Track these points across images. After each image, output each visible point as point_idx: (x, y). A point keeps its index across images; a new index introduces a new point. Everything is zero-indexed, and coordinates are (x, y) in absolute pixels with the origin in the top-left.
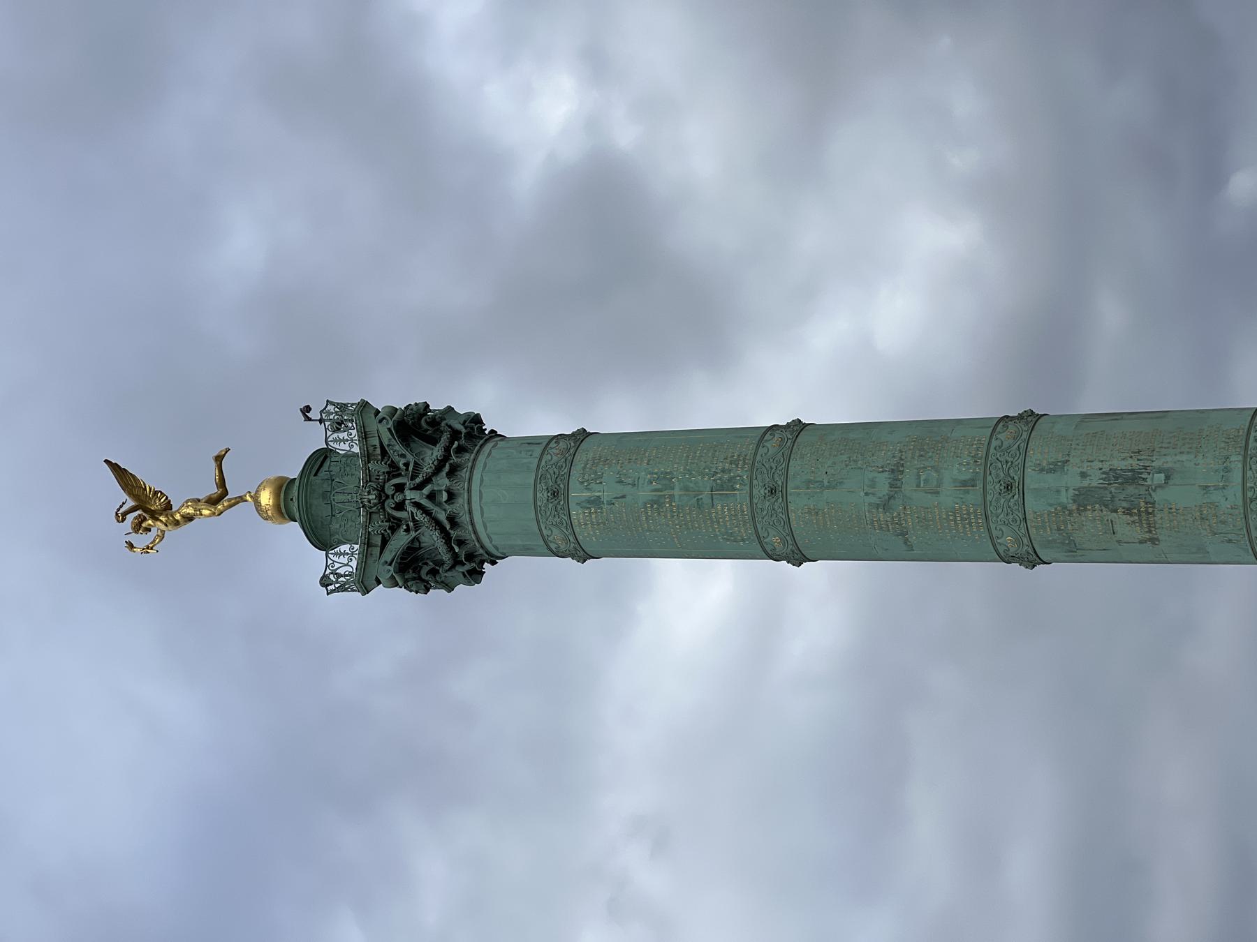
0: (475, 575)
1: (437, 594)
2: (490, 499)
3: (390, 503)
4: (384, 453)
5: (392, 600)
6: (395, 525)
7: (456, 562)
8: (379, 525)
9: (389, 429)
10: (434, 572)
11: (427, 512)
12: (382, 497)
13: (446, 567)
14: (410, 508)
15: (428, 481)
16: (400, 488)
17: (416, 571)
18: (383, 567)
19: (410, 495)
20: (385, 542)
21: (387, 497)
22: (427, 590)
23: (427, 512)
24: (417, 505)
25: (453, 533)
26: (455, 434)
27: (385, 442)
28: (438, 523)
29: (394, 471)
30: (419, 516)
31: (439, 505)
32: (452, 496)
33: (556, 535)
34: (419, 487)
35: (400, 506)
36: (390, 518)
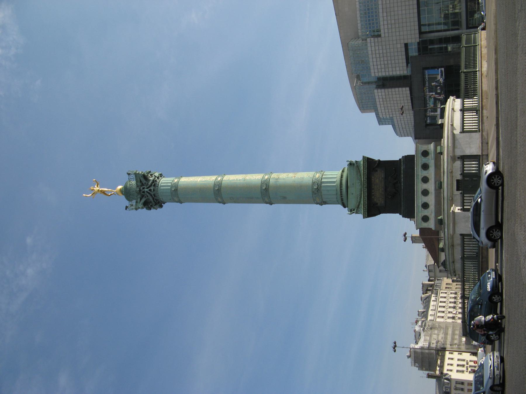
0: (161, 206)
1: (153, 210)
3: (141, 192)
4: (141, 181)
5: (144, 211)
6: (143, 196)
7: (156, 204)
8: (139, 196)
10: (152, 206)
11: (149, 193)
12: (140, 190)
15: (150, 187)
16: (144, 188)
17: (148, 205)
18: (140, 205)
19: (146, 190)
20: (141, 200)
22: (150, 209)
23: (149, 193)
24: (147, 192)
25: (155, 198)
26: (155, 177)
28: (151, 195)
29: (142, 185)
30: (148, 194)
32: (154, 190)
33: (176, 199)
34: (147, 188)
35: (144, 192)
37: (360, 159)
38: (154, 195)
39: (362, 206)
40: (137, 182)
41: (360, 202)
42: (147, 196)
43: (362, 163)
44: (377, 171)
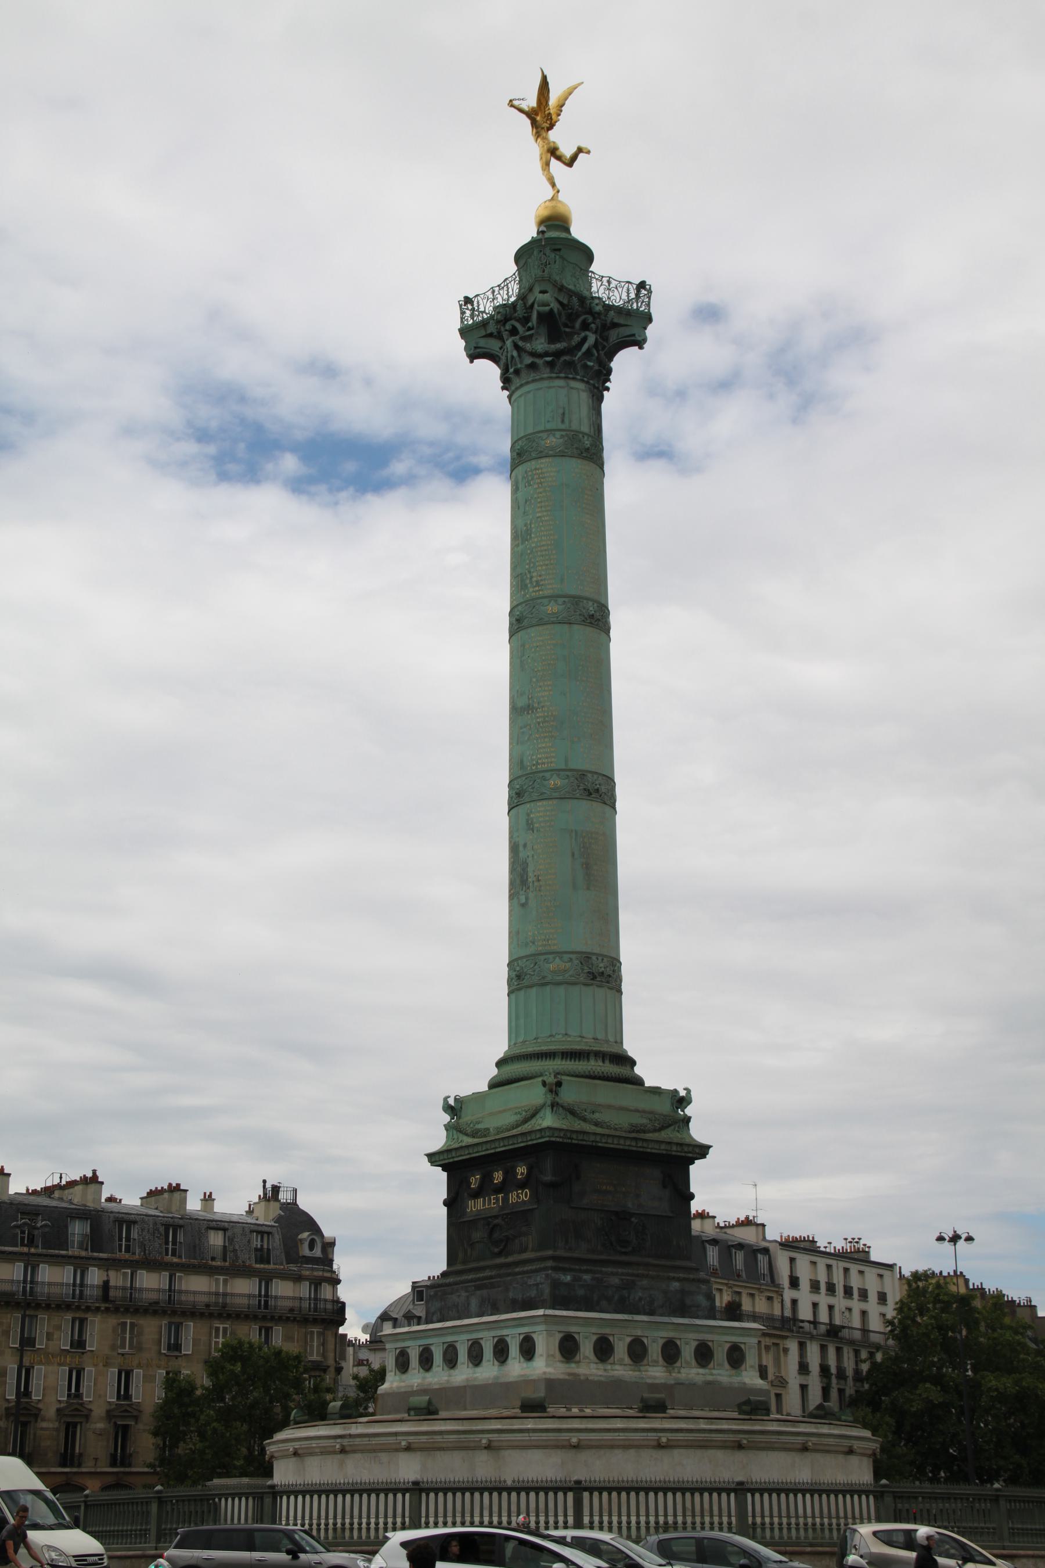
2: (562, 393)
3: (590, 319)
4: (615, 325)
9: (634, 335)
10: (514, 332)
12: (595, 315)
13: (521, 344)
14: (583, 334)
19: (592, 338)
21: (594, 318)
24: (584, 340)
27: (621, 329)
30: (577, 339)
31: (580, 359)
32: (586, 366)
35: (585, 326)
36: (578, 316)
37: (698, 1132)
38: (570, 365)
39: (578, 1125)
40: (619, 310)
41: (585, 1120)
42: (569, 336)
43: (687, 1141)
44: (665, 1187)
